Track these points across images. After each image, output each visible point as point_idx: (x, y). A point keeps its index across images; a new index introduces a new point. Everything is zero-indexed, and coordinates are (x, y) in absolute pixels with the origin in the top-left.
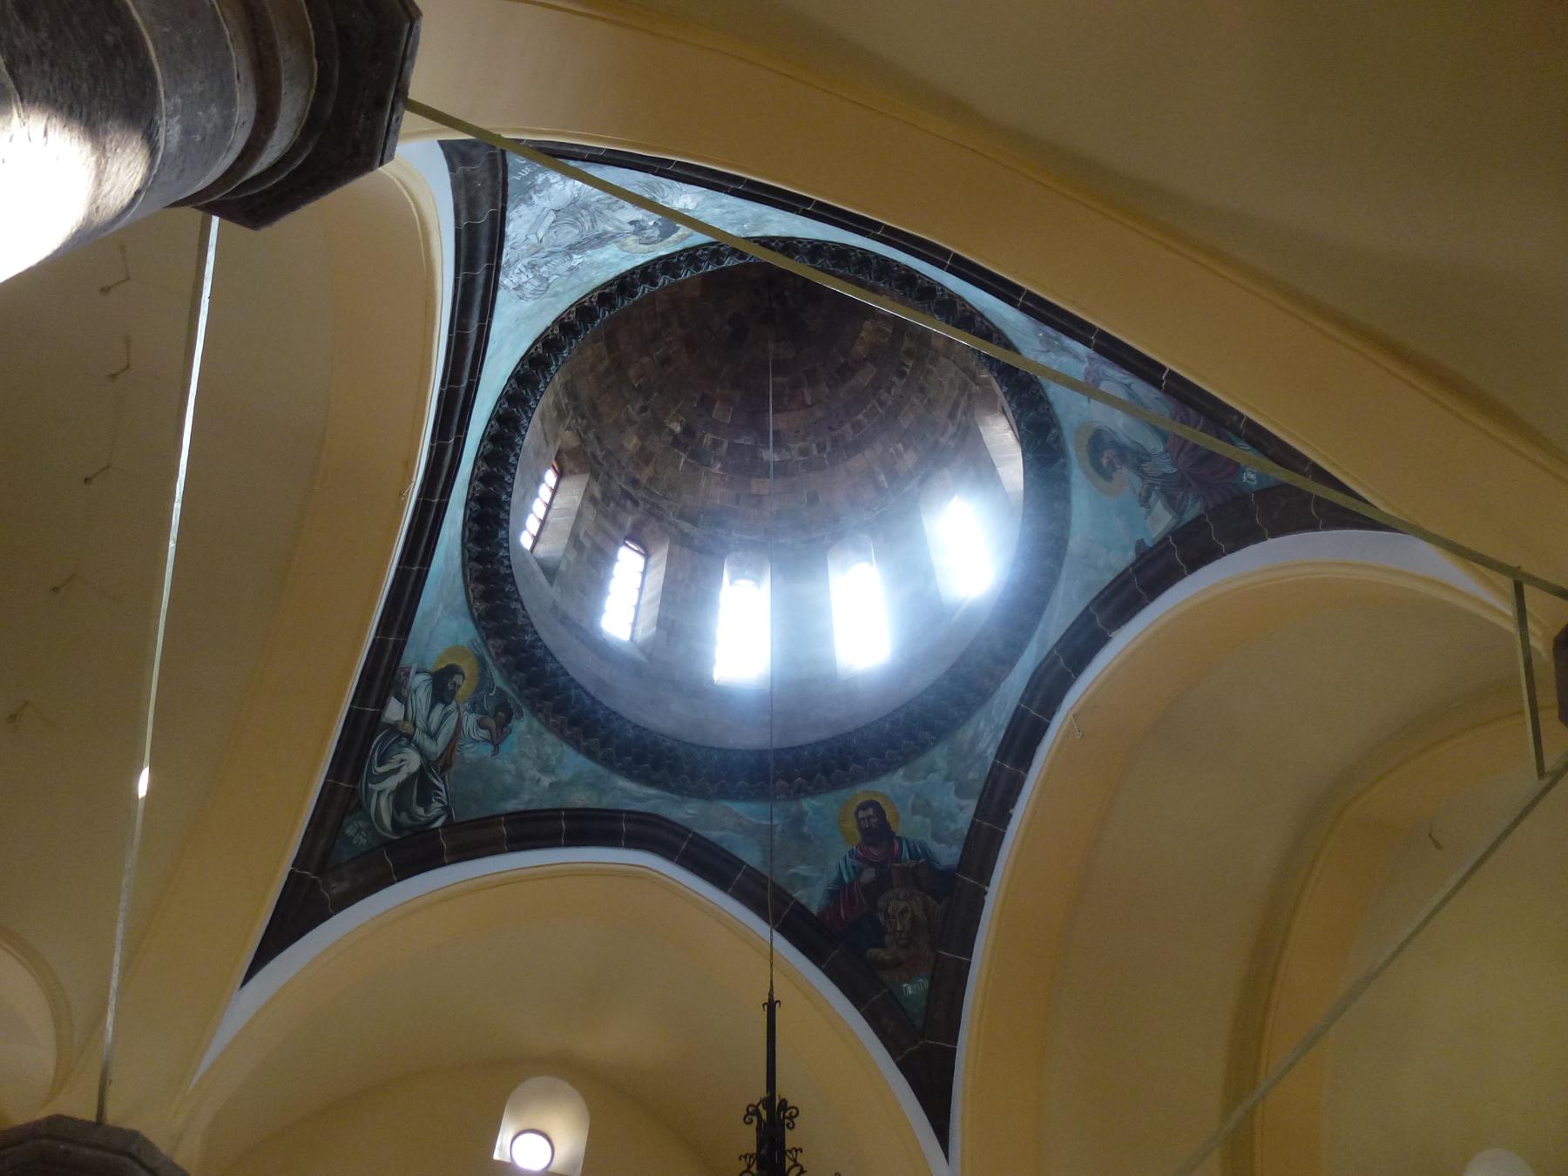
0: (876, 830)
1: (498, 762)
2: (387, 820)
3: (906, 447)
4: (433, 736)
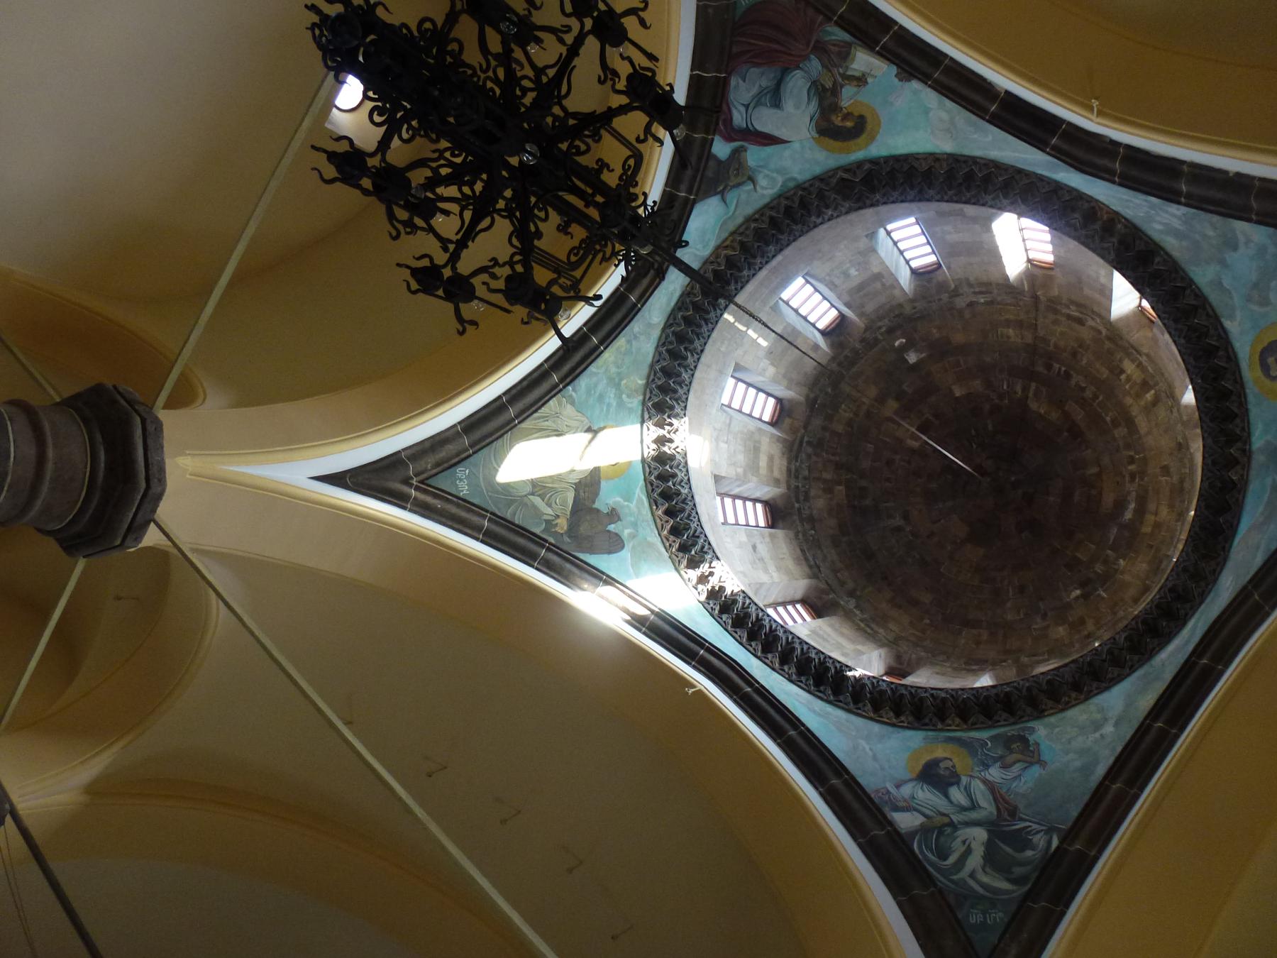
2: (1004, 885)
3: (1122, 371)
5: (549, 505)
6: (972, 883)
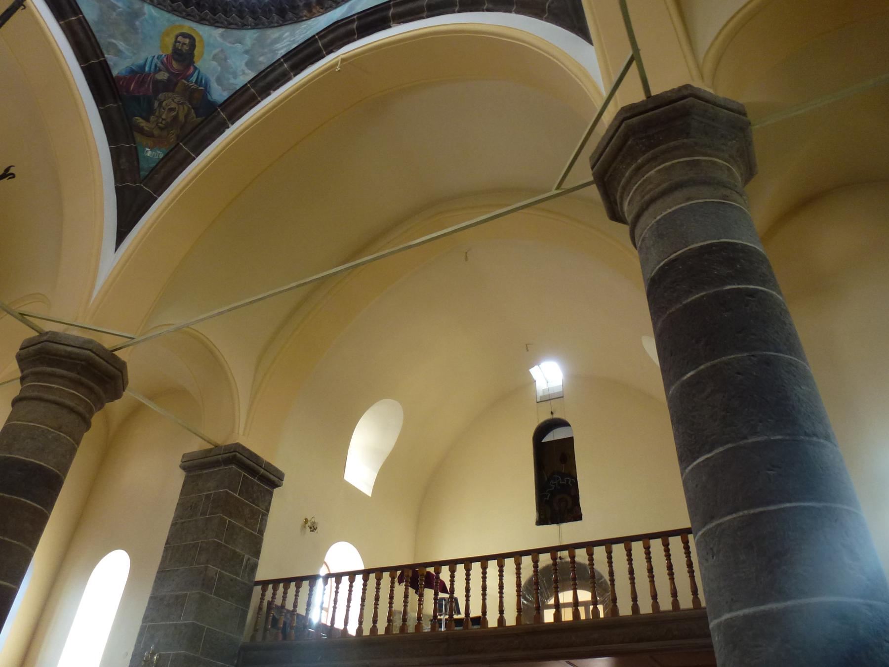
0: (184, 54)
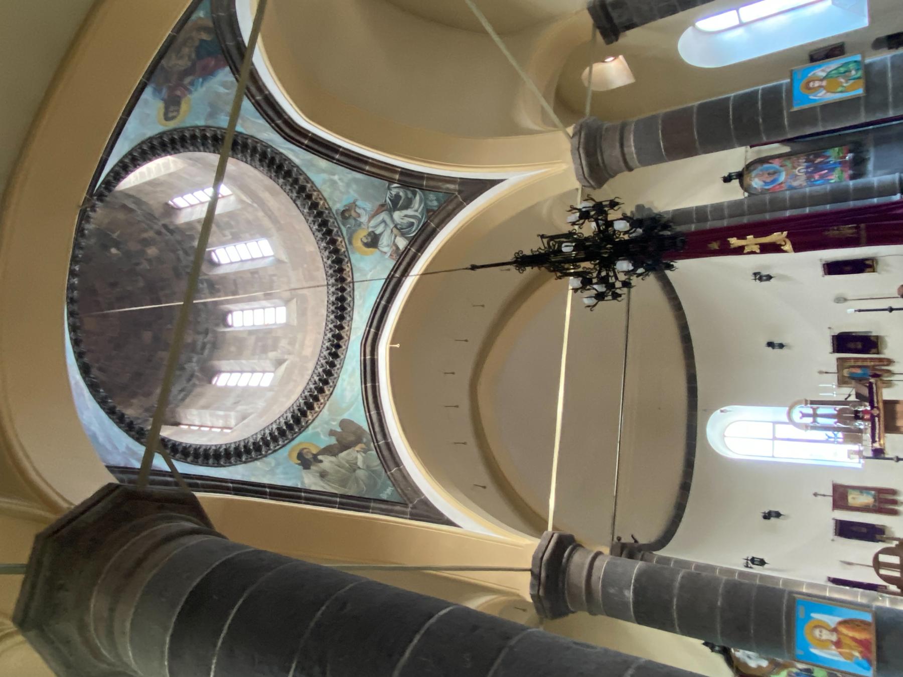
1: (356, 196)
2: (418, 198)
4: (384, 221)
5: (356, 458)
6: (420, 210)
